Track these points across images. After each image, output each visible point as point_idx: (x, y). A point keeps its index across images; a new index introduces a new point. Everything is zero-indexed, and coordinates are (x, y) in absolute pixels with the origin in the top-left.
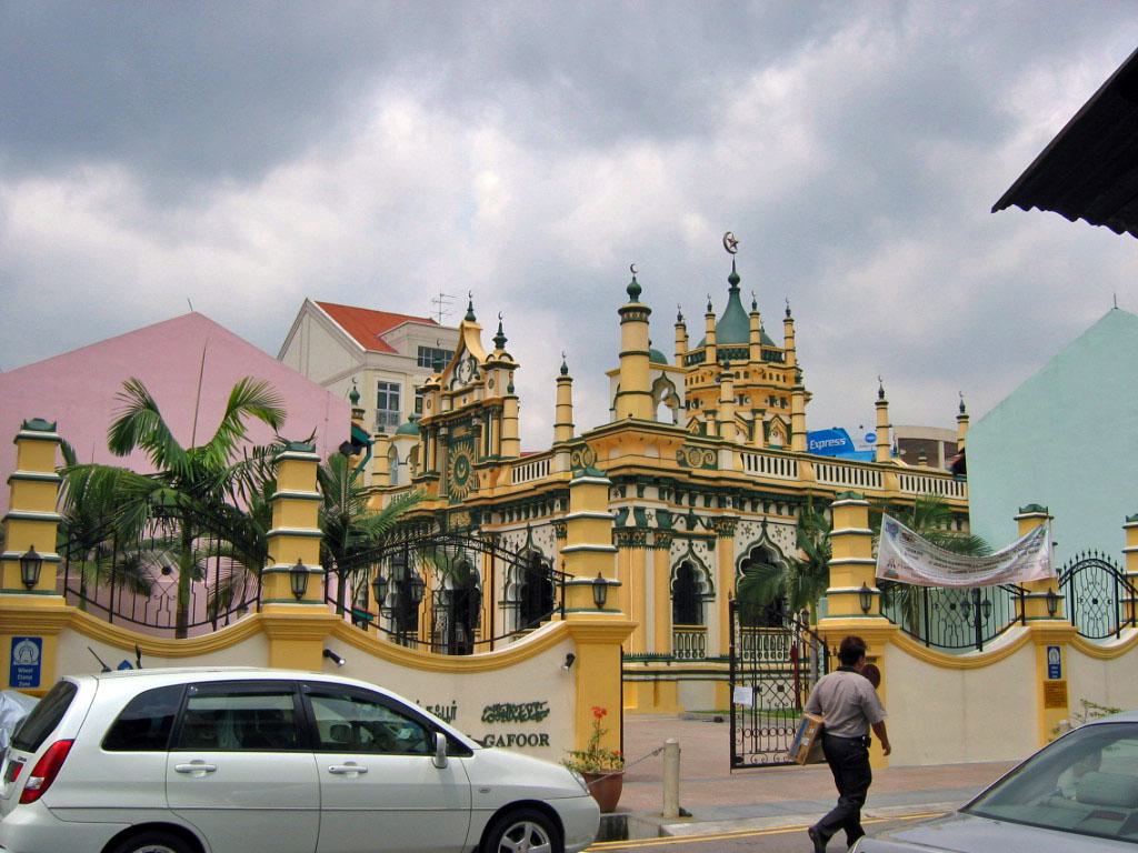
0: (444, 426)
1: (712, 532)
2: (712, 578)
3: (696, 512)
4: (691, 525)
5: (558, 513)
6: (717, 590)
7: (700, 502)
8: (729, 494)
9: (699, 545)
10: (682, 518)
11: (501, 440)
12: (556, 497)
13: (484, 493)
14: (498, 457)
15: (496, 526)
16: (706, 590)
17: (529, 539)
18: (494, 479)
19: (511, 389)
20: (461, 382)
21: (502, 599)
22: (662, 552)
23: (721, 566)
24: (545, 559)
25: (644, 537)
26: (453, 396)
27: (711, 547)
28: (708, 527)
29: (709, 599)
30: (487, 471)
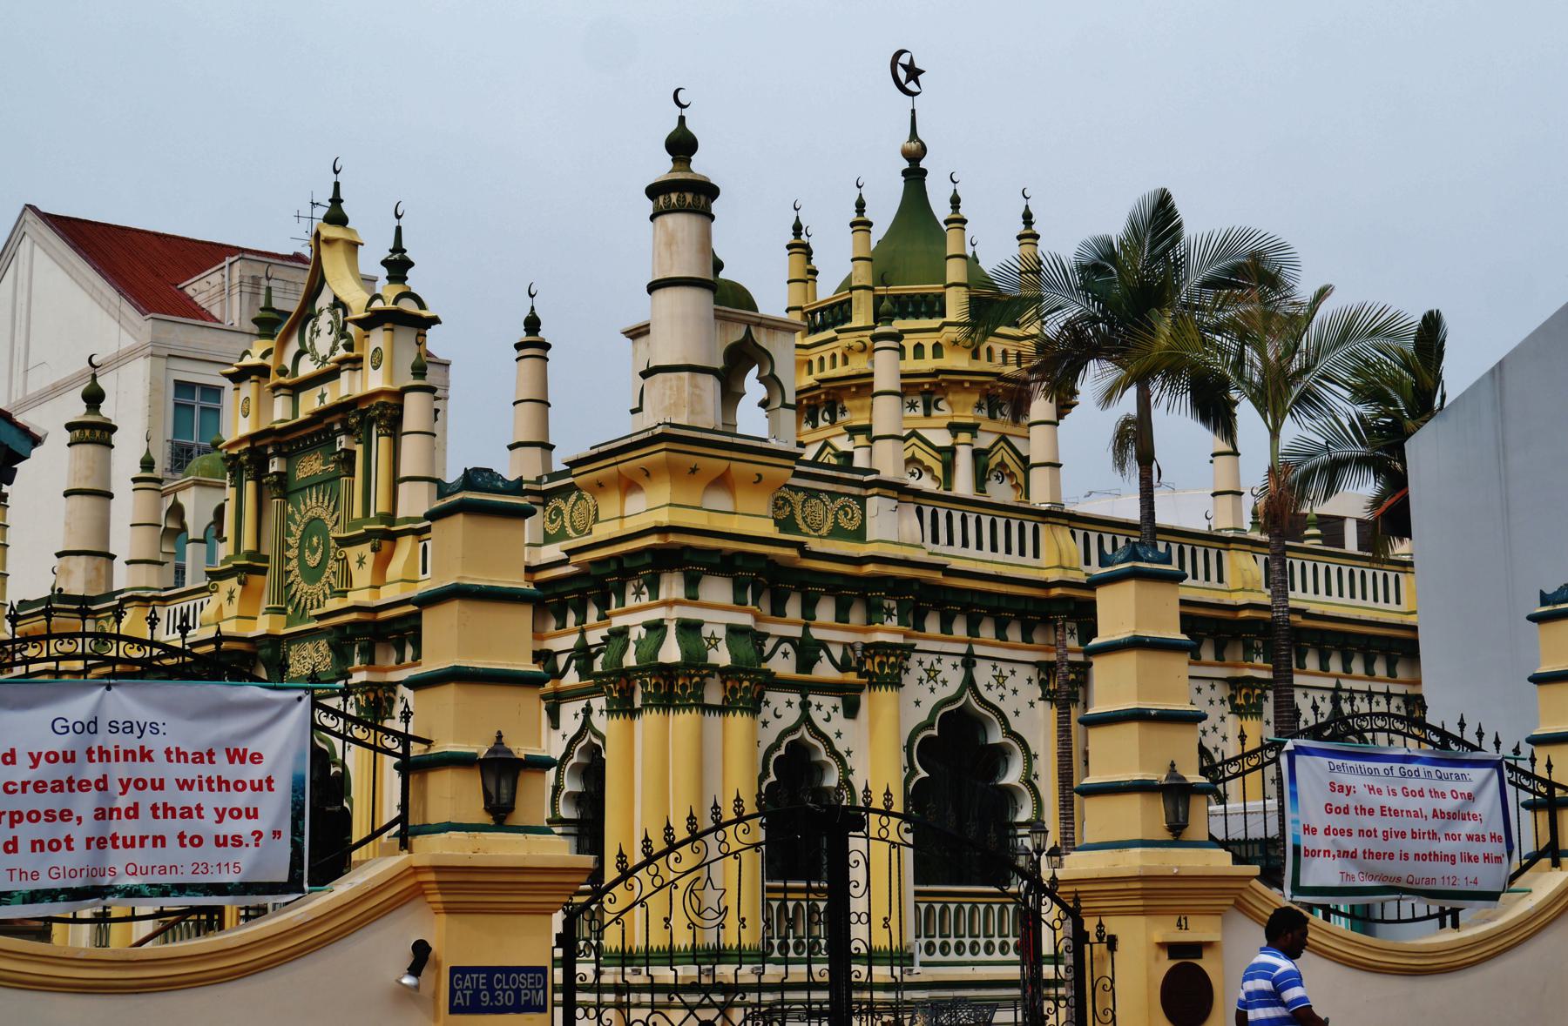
0: (278, 453)
1: (852, 677)
4: (805, 664)
7: (826, 611)
8: (891, 594)
9: (825, 708)
10: (786, 646)
13: (360, 596)
15: (386, 670)
18: (382, 564)
23: (873, 752)
27: (851, 711)
28: (843, 667)
30: (365, 549)
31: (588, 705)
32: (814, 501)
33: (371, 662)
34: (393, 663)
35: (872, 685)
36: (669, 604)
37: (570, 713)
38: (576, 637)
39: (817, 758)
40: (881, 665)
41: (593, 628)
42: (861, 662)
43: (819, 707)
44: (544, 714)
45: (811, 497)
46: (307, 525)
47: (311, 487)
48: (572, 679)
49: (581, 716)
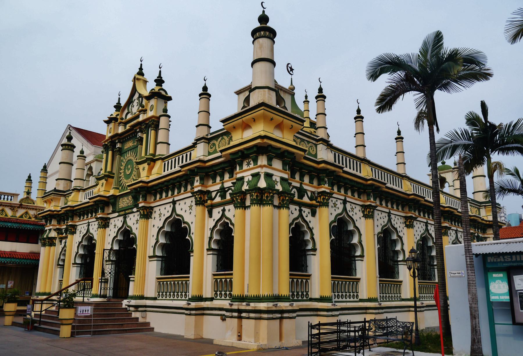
0: (119, 142)
1: (314, 202)
2: (315, 237)
3: (305, 187)
5: (197, 187)
6: (318, 246)
7: (306, 179)
8: (327, 176)
9: (306, 211)
10: (294, 190)
11: (156, 143)
12: (197, 175)
14: (154, 155)
15: (150, 203)
16: (310, 247)
17: (174, 210)
19: (165, 110)
20: (132, 114)
21: (152, 254)
22: (284, 212)
24: (185, 223)
25: (273, 197)
26: (125, 124)
27: (314, 214)
28: (311, 199)
29: (312, 253)
30: (146, 165)
31: (224, 208)
32: (303, 143)
33: (146, 200)
34: (152, 200)
35: (320, 206)
36: (261, 166)
37: (217, 213)
38: (220, 185)
39: (303, 230)
40: (324, 199)
41: (227, 181)
42: (317, 198)
43: (304, 212)
44: (207, 212)
45: (302, 141)
46: (127, 162)
47: (129, 151)
48: (218, 199)
49: (221, 213)
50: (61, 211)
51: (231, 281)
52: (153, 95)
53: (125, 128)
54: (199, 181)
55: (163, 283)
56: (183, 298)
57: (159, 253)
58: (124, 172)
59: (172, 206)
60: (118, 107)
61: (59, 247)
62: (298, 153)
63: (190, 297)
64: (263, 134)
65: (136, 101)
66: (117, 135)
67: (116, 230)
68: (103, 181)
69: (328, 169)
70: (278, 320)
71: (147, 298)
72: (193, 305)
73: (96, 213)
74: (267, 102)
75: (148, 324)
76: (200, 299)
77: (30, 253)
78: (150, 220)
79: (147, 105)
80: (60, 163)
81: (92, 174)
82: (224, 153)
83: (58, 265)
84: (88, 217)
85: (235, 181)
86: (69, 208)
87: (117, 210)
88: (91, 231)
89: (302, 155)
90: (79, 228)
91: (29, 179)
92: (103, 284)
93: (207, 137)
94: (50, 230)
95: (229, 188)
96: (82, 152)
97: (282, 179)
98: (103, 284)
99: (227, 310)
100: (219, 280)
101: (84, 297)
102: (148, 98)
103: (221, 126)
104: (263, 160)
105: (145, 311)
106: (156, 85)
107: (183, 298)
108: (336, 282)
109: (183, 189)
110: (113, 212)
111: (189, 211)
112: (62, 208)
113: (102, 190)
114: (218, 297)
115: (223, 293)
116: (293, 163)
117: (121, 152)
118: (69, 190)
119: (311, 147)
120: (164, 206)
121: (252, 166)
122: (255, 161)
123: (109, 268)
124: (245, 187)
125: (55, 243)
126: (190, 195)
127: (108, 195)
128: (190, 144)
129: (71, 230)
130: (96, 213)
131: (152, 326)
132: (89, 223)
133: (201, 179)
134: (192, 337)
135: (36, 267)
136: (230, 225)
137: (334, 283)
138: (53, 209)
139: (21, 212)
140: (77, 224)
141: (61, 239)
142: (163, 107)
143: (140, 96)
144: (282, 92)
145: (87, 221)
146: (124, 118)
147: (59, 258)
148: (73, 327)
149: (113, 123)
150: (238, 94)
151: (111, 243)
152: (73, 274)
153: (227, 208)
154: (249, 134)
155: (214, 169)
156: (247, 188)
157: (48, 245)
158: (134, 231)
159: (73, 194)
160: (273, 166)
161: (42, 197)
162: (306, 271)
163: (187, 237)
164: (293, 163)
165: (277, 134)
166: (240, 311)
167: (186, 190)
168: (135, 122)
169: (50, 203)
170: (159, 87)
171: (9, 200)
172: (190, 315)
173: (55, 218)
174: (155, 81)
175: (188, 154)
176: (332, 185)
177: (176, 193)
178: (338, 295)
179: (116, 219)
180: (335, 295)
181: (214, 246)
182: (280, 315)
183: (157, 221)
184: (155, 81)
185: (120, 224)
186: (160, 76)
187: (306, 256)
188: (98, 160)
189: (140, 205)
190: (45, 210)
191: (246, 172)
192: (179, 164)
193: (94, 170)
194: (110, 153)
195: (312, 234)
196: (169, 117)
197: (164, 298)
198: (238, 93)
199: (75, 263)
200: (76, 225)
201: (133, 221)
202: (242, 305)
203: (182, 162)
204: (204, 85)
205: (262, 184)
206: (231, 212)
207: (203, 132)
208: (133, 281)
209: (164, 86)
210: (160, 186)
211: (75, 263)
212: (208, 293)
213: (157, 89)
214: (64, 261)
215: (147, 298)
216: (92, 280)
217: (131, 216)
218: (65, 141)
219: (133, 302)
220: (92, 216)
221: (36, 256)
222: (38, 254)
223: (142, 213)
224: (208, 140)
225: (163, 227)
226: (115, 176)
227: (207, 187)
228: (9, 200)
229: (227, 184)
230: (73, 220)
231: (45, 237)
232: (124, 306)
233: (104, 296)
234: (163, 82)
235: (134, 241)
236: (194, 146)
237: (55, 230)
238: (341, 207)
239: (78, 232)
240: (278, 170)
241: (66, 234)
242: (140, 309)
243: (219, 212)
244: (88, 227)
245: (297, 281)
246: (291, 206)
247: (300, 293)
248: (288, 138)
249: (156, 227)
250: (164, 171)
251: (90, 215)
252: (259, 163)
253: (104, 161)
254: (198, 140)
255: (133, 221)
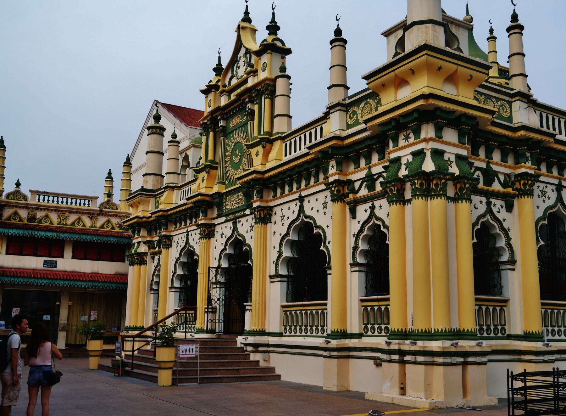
0: (222, 118)
1: (510, 190)
2: (513, 242)
3: (495, 168)
5: (333, 175)
6: (518, 257)
7: (497, 156)
8: (528, 150)
9: (498, 204)
10: (478, 173)
11: (273, 117)
12: (331, 158)
14: (270, 133)
15: (268, 201)
16: (505, 257)
17: (301, 210)
20: (237, 78)
21: (273, 273)
22: (464, 206)
25: (445, 185)
26: (229, 93)
27: (509, 208)
28: (504, 185)
29: (509, 267)
30: (260, 149)
31: (373, 204)
32: (489, 101)
33: (262, 197)
34: (271, 198)
36: (426, 140)
37: (363, 212)
39: (493, 232)
40: (525, 185)
41: (375, 165)
43: (495, 205)
44: (348, 211)
45: (487, 98)
46: (234, 146)
47: (235, 130)
48: (364, 192)
49: (369, 211)
50: (151, 217)
51: (387, 310)
52: (266, 48)
53: (230, 98)
54: (335, 167)
55: (291, 314)
56: (320, 334)
57: (283, 271)
58: (231, 160)
59: (298, 205)
60: (218, 70)
61: (151, 266)
62: (481, 117)
63: (329, 332)
64: (427, 91)
65: (243, 59)
66: (219, 109)
67: (224, 240)
68: (204, 174)
69: (530, 139)
70: (460, 367)
71: (270, 334)
72: (334, 343)
73: (196, 219)
74: (431, 43)
75: (273, 369)
76: (343, 335)
77: (116, 274)
78: (269, 224)
79: (257, 63)
80: (147, 153)
81: (188, 166)
82: (369, 124)
83: (152, 289)
84: (186, 224)
85: (387, 164)
86: (161, 213)
87: (224, 213)
88: (191, 243)
89: (488, 120)
90: (175, 239)
91: (109, 177)
92: (210, 315)
93: (343, 102)
94: (139, 243)
95: (380, 175)
96: (174, 136)
97: (459, 157)
98: (210, 315)
99: (383, 351)
100: (369, 308)
101: (186, 332)
102: (259, 54)
103: (363, 85)
104: (428, 131)
105: (268, 352)
106: (269, 34)
107: (320, 334)
108: (549, 311)
109: (312, 180)
110: (219, 216)
111: (322, 210)
112: (152, 214)
113: (203, 186)
114: (369, 333)
115: (376, 326)
116: (474, 133)
117: (225, 132)
118: (160, 189)
119: (502, 106)
120: (287, 206)
121: (412, 140)
122: (417, 133)
123: (216, 293)
124: (403, 172)
125: (146, 261)
126: (323, 187)
127: (211, 193)
128: (320, 114)
129: (165, 242)
130: (196, 219)
131: (278, 372)
132: (188, 232)
133: (337, 164)
134: (335, 389)
135: (123, 293)
136: (382, 229)
137: (546, 312)
138: (140, 214)
139: (101, 220)
140: (173, 234)
141: (153, 255)
142: (280, 64)
143: (248, 51)
144: (454, 26)
145: (185, 230)
146: (227, 84)
147: (152, 280)
148: (174, 373)
149: (213, 93)
150: (386, 36)
151: (217, 259)
152: (171, 302)
153: (377, 203)
154: (405, 94)
155: (357, 148)
156: (406, 173)
157: (137, 264)
158: (248, 241)
159: (165, 194)
160: (444, 139)
161: (127, 200)
162: (501, 294)
163: (322, 248)
164: (474, 133)
165: (449, 91)
166: (402, 353)
167: (318, 181)
168: (242, 88)
169: (137, 207)
170: (273, 37)
171: (87, 205)
172: (330, 357)
173: (144, 227)
174: (268, 28)
175: (319, 129)
176: (537, 163)
177: (303, 186)
178: (553, 331)
179: (223, 226)
180: (548, 330)
181: (360, 259)
182: (462, 360)
183: (278, 227)
184: (268, 28)
185: (228, 233)
186: (273, 21)
187: (499, 271)
188: (196, 145)
189: (255, 205)
190: (131, 217)
191: (403, 150)
192: (305, 144)
193: (191, 160)
194: (211, 134)
195: (508, 239)
196: (289, 77)
197: (293, 334)
198: (387, 34)
199: (172, 287)
200: (172, 236)
201: (246, 227)
202: (404, 344)
203: (310, 141)
204: (336, 27)
205: (429, 166)
206: (384, 209)
207: (338, 96)
208: (250, 310)
209: (280, 34)
210: (281, 176)
211: (172, 287)
212: (354, 326)
213: (270, 39)
214: (158, 284)
215: (270, 334)
216: (195, 309)
217: (243, 220)
218: (152, 122)
219: (251, 340)
220: (191, 223)
221: (123, 278)
222: (126, 276)
223: (258, 216)
224: (345, 107)
225: (287, 234)
226: (219, 166)
227: (347, 175)
228: (87, 205)
229: (376, 170)
230: (167, 229)
231: (133, 252)
232: (239, 345)
233: (212, 331)
234: (279, 28)
235: (248, 255)
236: (326, 116)
237: (144, 243)
238: (553, 196)
239: (174, 245)
240: (452, 145)
241: (159, 248)
242: (261, 349)
243: (366, 211)
244: (187, 238)
245: (487, 309)
246: (473, 197)
247: (492, 328)
248: (466, 95)
249: (277, 234)
250: (286, 155)
251: (188, 221)
252: (423, 136)
253: (203, 146)
254: (331, 108)
255: (246, 227)
